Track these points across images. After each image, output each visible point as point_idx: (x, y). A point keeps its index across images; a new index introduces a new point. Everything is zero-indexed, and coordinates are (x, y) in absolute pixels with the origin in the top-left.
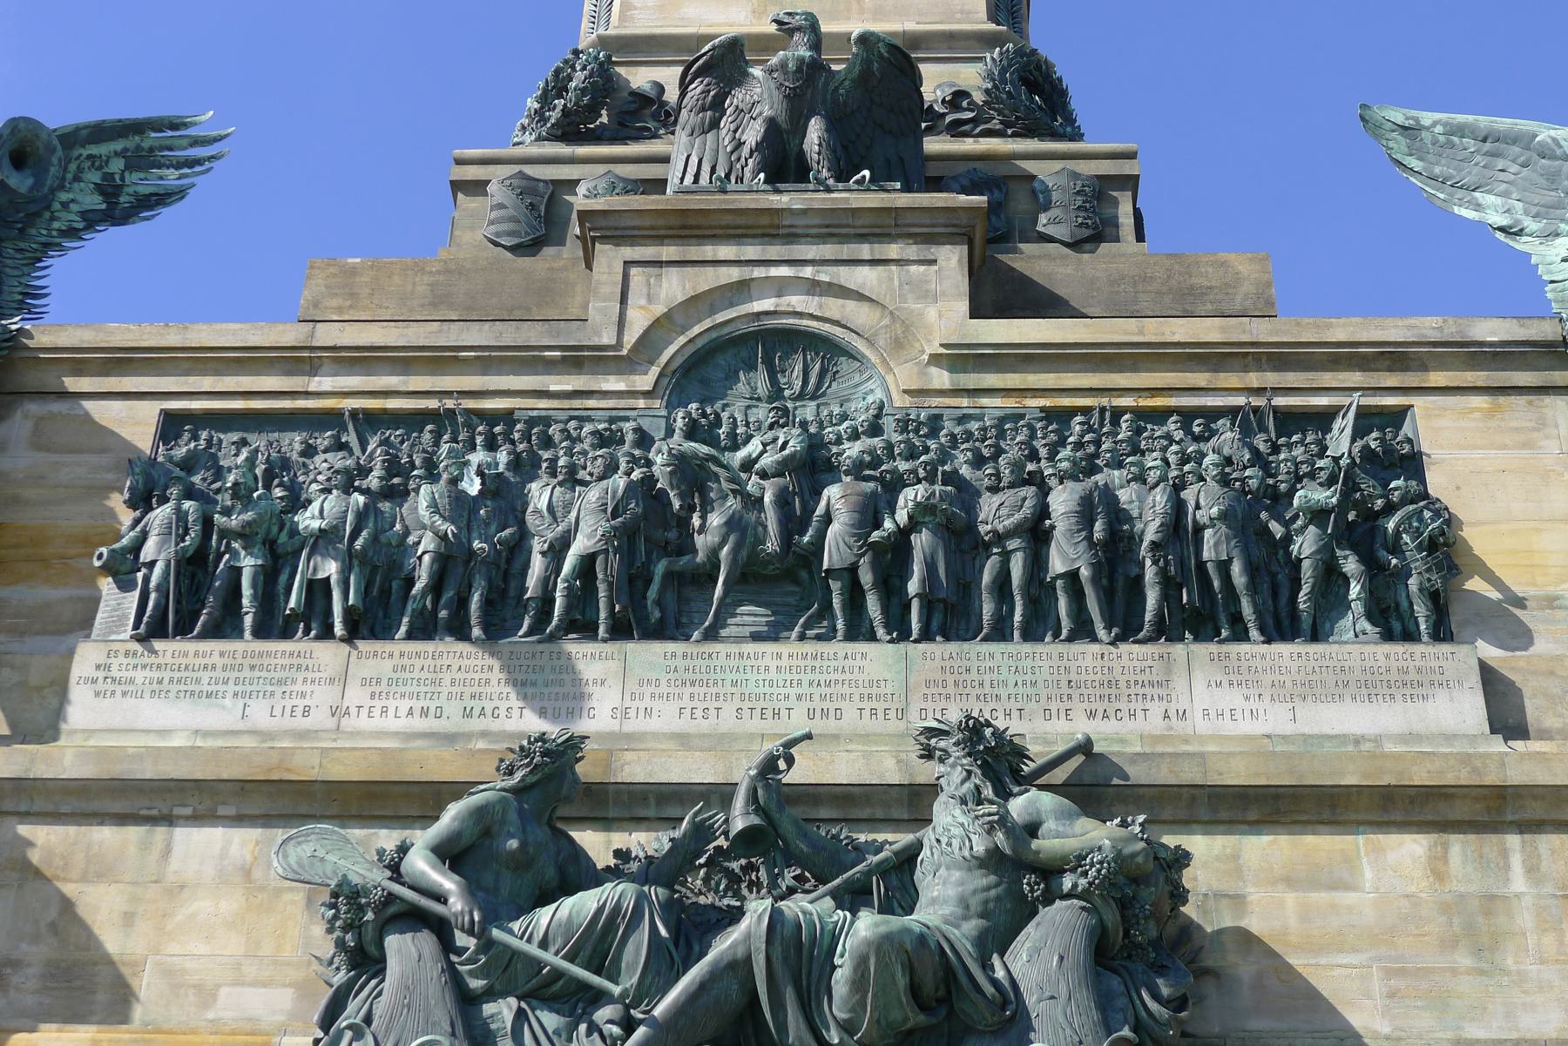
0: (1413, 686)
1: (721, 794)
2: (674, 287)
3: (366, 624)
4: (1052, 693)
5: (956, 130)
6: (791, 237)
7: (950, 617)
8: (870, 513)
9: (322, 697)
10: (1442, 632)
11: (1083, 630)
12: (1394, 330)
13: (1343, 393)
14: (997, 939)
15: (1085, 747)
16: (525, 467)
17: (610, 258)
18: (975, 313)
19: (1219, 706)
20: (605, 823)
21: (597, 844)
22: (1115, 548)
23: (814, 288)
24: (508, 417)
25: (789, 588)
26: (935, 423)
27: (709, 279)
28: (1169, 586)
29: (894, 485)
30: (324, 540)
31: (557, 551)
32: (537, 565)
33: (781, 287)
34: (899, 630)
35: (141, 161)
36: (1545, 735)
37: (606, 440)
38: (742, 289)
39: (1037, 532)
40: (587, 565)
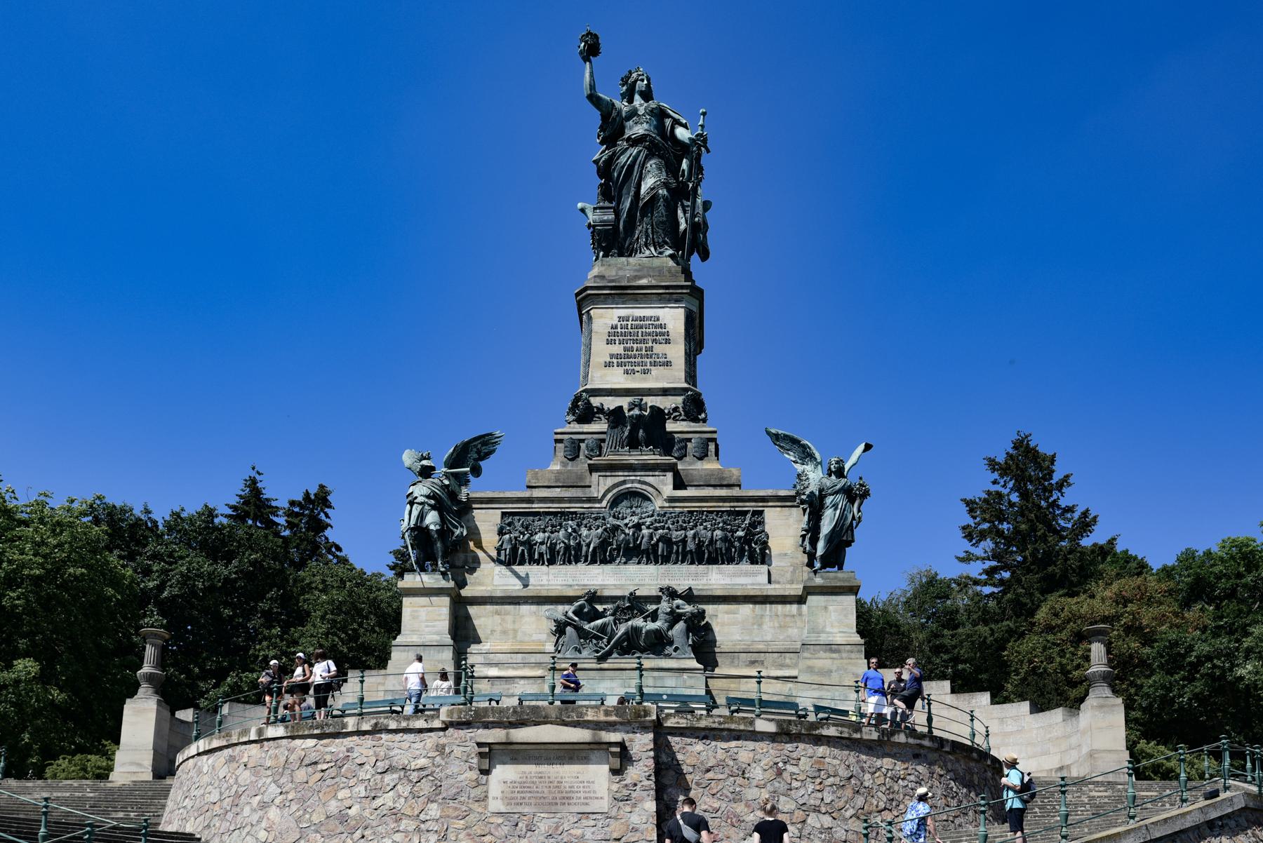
0: (754, 574)
1: (622, 598)
2: (610, 481)
3: (552, 562)
4: (684, 576)
5: (675, 419)
6: (635, 470)
7: (666, 560)
8: (651, 537)
9: (545, 578)
10: (763, 563)
11: (692, 563)
12: (762, 493)
13: (750, 507)
14: (671, 627)
15: (690, 589)
16: (579, 525)
17: (595, 475)
18: (675, 488)
19: (715, 578)
20: (601, 603)
21: (600, 608)
22: (700, 545)
23: (640, 482)
24: (575, 513)
25: (634, 552)
26: (664, 515)
27: (617, 480)
28: (710, 553)
29: (656, 529)
30: (542, 543)
31: (588, 545)
32: (584, 549)
33: (633, 482)
34: (656, 562)
35: (485, 444)
36: (779, 583)
37: (596, 519)
38: (624, 482)
39: (684, 541)
40: (595, 548)
